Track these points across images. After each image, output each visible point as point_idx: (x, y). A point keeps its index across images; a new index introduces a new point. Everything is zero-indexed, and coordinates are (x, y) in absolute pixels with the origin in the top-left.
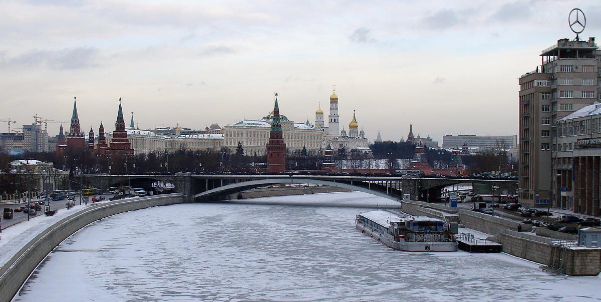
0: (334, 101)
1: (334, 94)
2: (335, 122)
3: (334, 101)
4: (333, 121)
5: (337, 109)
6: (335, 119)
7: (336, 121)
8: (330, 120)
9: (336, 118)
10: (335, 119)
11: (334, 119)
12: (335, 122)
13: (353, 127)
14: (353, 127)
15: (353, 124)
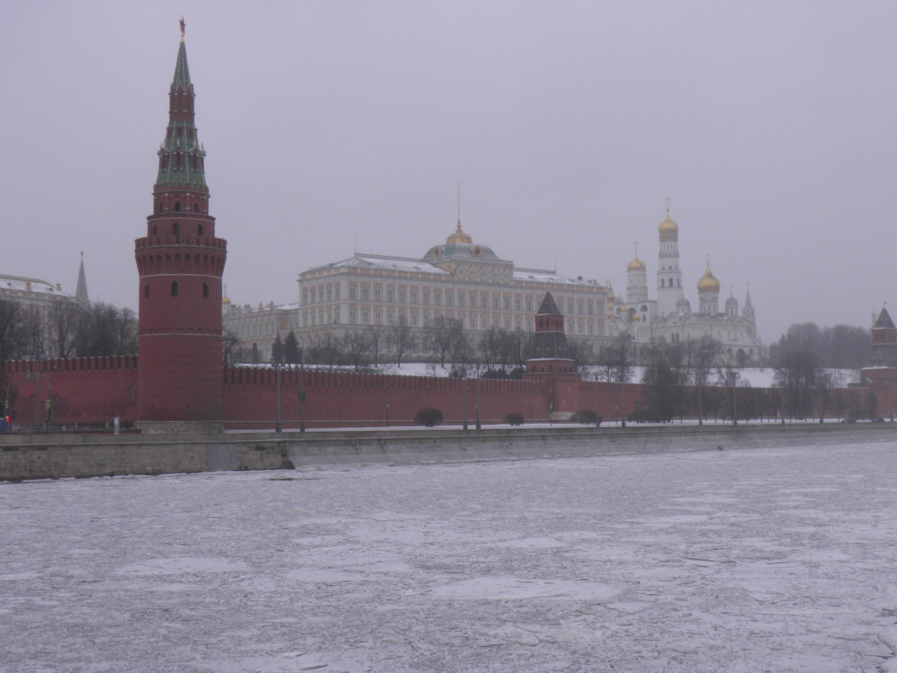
0: (669, 234)
1: (669, 221)
2: (671, 285)
3: (669, 234)
4: (667, 284)
5: (676, 255)
6: (671, 280)
7: (675, 283)
8: (660, 286)
9: (675, 277)
10: (671, 280)
11: (672, 283)
12: (671, 285)
13: (709, 290)
14: (709, 290)
15: (707, 282)
